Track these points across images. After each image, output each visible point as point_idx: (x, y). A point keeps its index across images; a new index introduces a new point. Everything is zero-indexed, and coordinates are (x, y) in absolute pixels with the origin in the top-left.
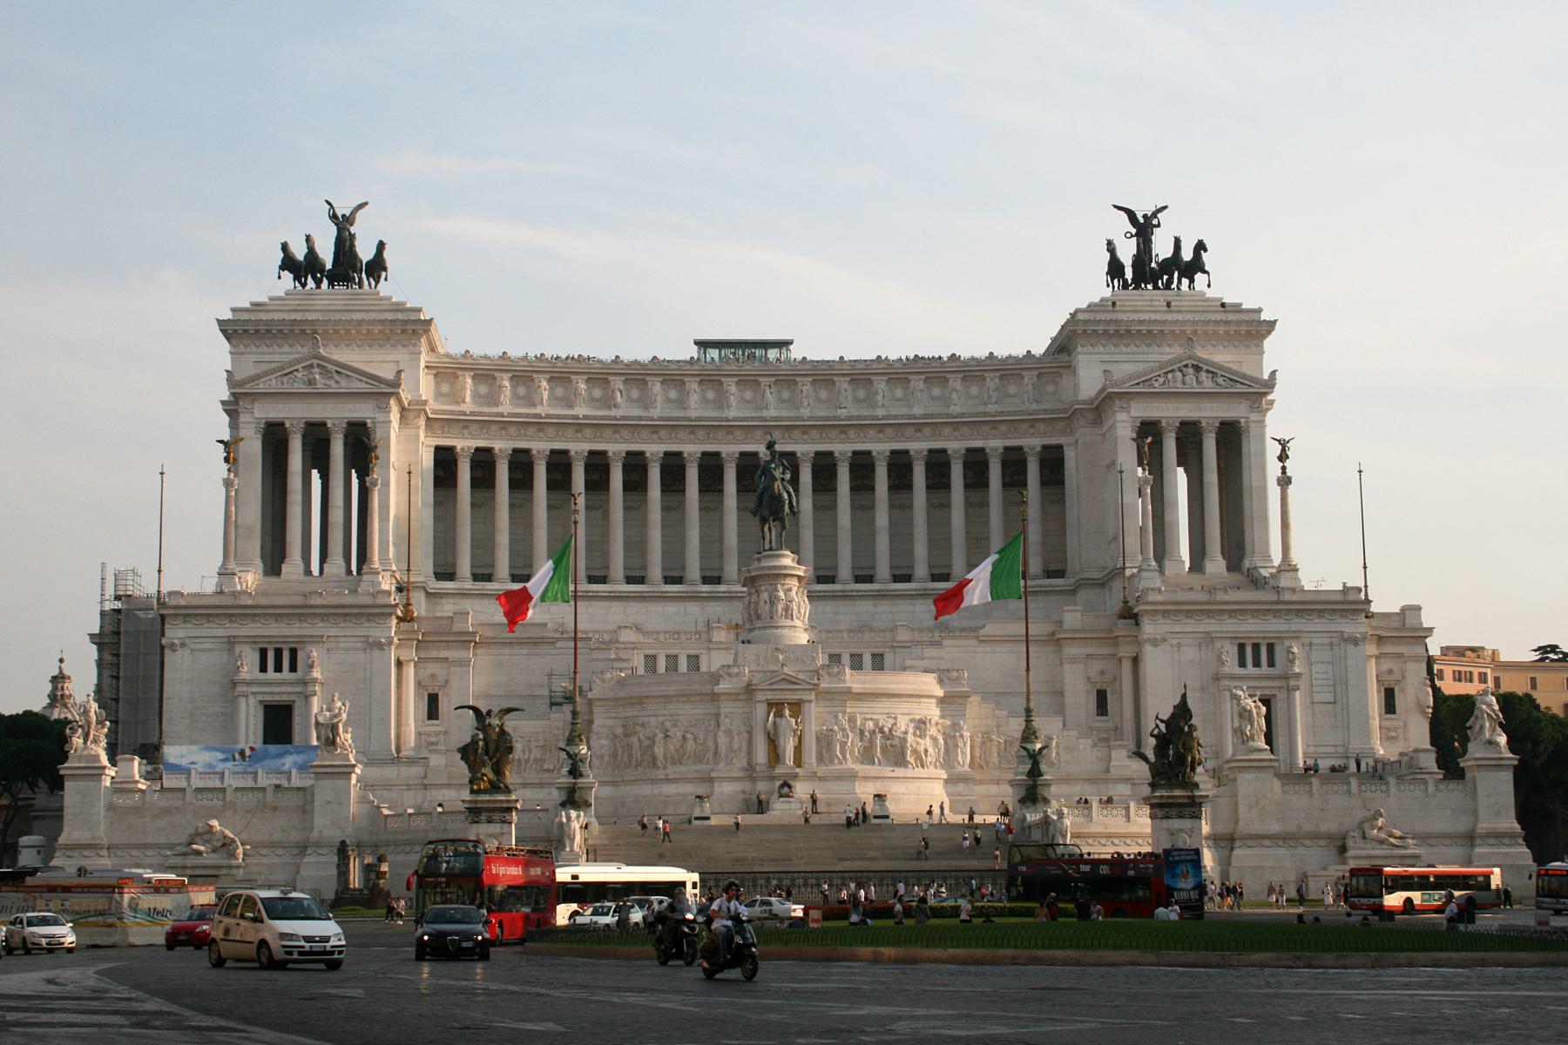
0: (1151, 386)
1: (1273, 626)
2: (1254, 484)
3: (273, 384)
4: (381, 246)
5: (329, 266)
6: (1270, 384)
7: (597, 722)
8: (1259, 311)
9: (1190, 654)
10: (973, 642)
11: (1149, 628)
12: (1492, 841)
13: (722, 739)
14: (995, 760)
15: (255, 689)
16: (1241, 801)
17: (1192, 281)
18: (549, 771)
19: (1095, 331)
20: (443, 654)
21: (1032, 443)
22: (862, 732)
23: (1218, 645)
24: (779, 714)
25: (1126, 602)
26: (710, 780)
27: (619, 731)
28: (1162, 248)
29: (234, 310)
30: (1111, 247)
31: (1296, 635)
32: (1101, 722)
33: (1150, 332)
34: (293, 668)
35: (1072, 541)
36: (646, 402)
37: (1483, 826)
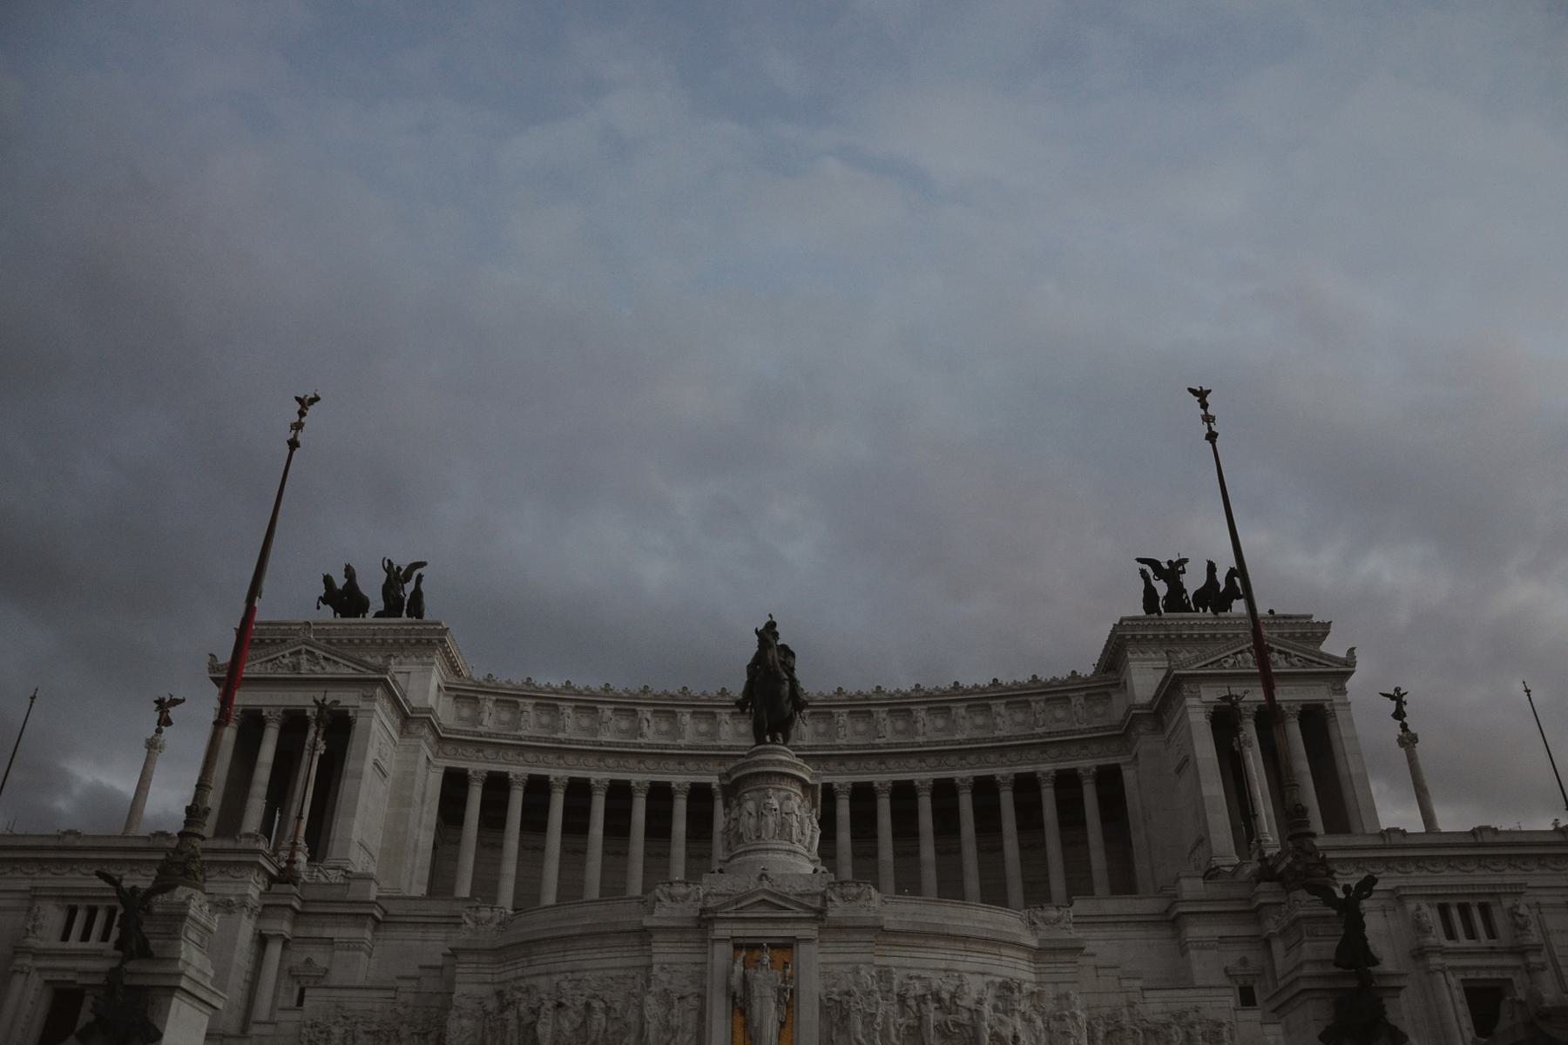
0: (1221, 667)
1: (1481, 878)
2: (1353, 771)
4: (420, 577)
5: (377, 603)
6: (1349, 663)
7: (459, 989)
13: (653, 1007)
19: (1145, 636)
20: (328, 932)
21: (1086, 764)
22: (902, 999)
23: (1411, 906)
25: (1263, 860)
27: (491, 1005)
28: (1193, 581)
33: (1201, 636)
35: (1141, 867)
36: (676, 731)
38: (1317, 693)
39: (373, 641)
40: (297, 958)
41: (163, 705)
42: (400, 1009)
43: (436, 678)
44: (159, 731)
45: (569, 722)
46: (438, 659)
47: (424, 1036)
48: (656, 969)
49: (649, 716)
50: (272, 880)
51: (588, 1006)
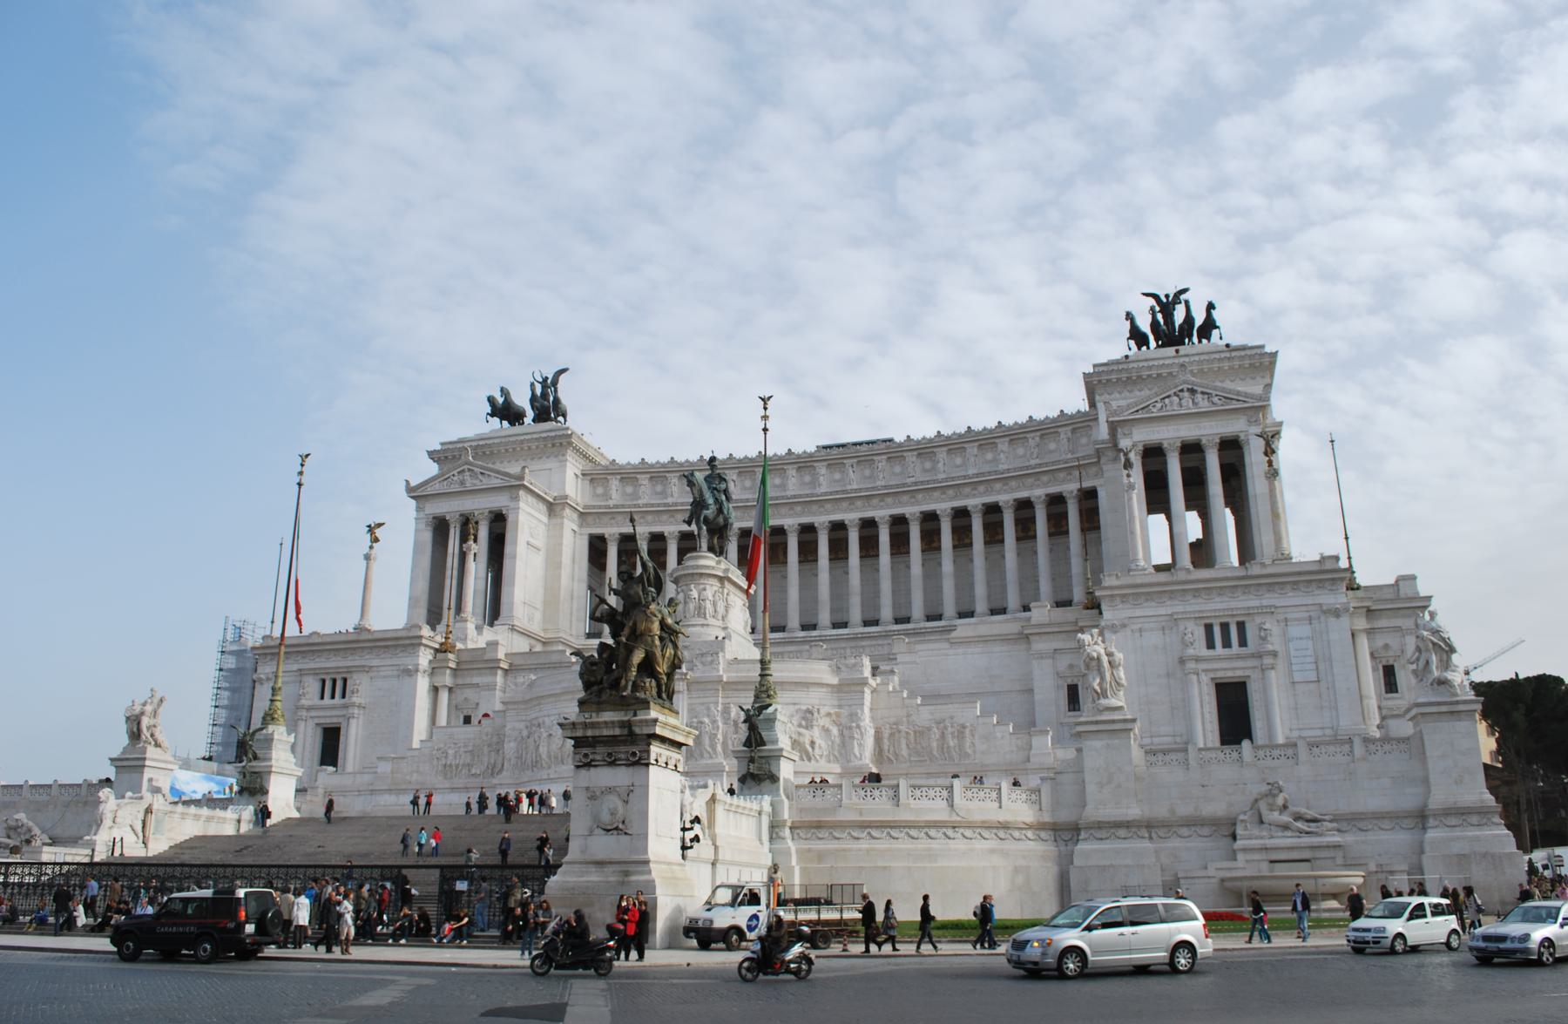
7: (509, 726)
8: (1262, 347)
9: (1154, 638)
10: (946, 645)
11: (1108, 614)
12: (1453, 821)
14: (905, 752)
16: (1088, 778)
20: (476, 680)
21: (1070, 488)
27: (525, 733)
28: (1179, 315)
30: (1129, 316)
31: (1270, 611)
32: (1072, 717)
33: (1159, 375)
37: (1437, 800)
40: (460, 696)
41: (371, 529)
45: (675, 489)
50: (437, 651)
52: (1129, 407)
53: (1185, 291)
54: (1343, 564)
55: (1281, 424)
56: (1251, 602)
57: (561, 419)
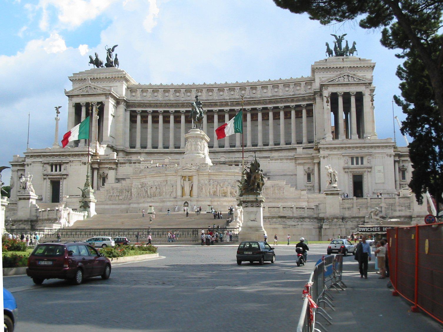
0: (333, 82)
3: (76, 93)
4: (116, 55)
5: (105, 62)
6: (372, 80)
7: (134, 184)
8: (371, 60)
15: (49, 177)
17: (353, 53)
18: (121, 200)
24: (184, 180)
26: (164, 202)
27: (140, 186)
28: (344, 45)
29: (74, 74)
30: (327, 45)
31: (370, 155)
33: (337, 67)
34: (60, 171)
38: (361, 89)
39: (106, 78)
41: (57, 109)
42: (123, 187)
43: (125, 87)
44: (57, 115)
46: (124, 82)
47: (128, 192)
48: (168, 181)
49: (184, 92)
50: (93, 155)
51: (156, 187)
52: (327, 80)
53: (345, 35)
54: (393, 141)
55: (375, 87)
56: (366, 151)
57: (117, 65)
